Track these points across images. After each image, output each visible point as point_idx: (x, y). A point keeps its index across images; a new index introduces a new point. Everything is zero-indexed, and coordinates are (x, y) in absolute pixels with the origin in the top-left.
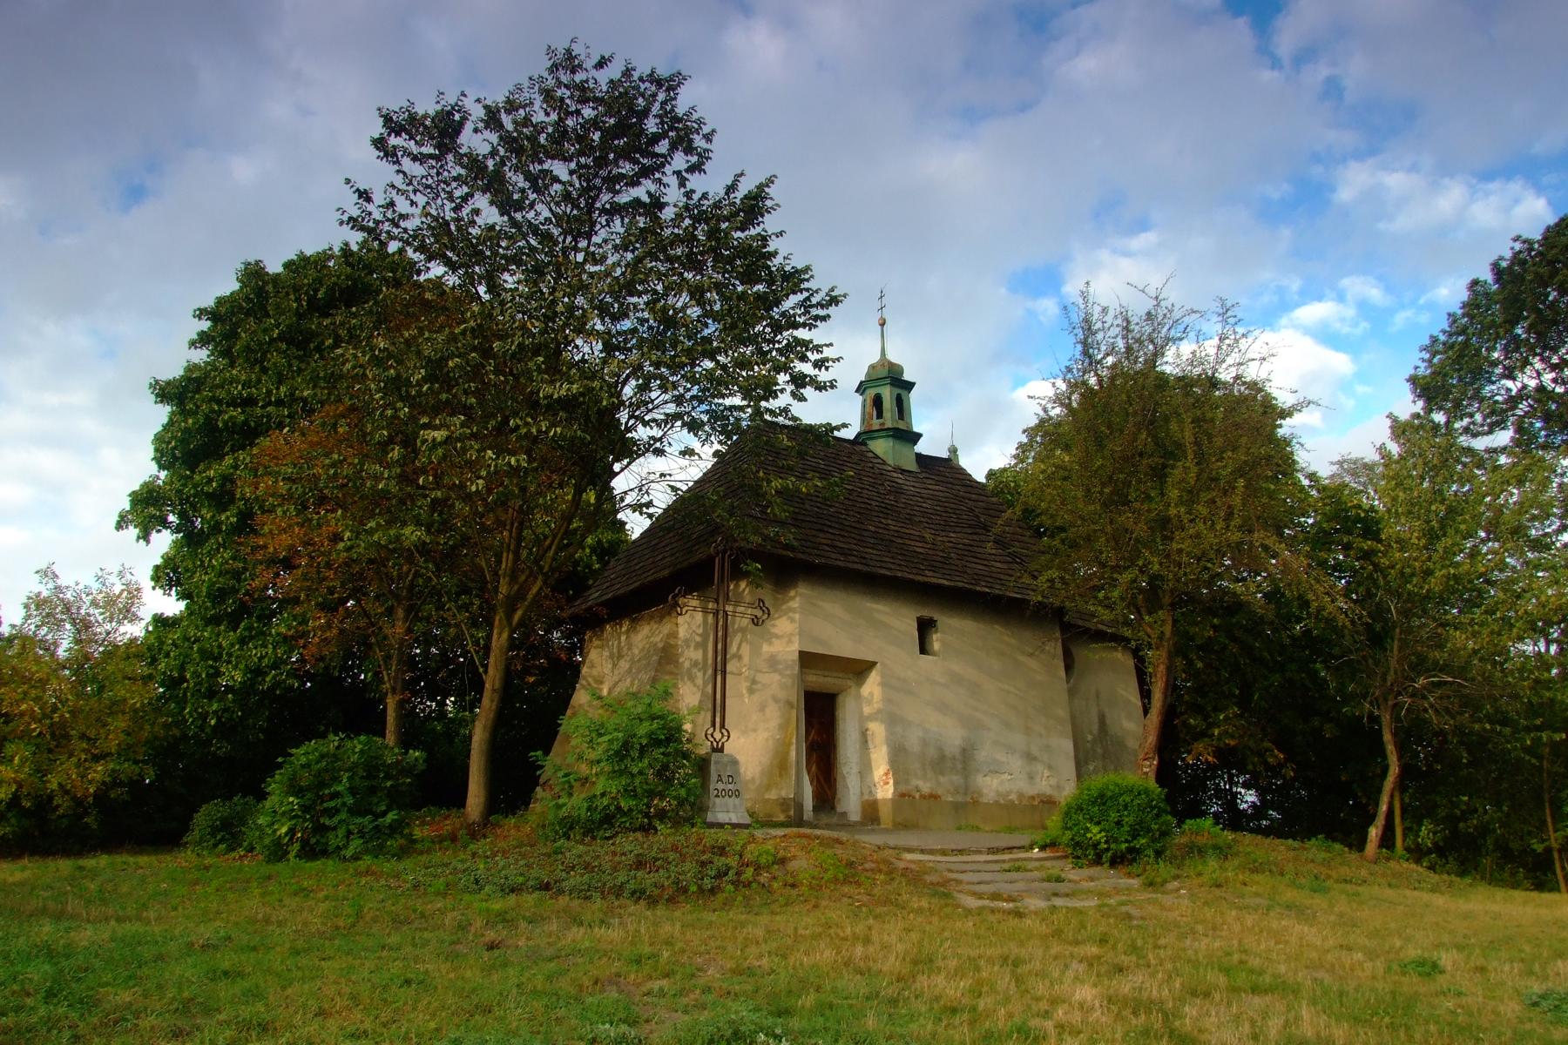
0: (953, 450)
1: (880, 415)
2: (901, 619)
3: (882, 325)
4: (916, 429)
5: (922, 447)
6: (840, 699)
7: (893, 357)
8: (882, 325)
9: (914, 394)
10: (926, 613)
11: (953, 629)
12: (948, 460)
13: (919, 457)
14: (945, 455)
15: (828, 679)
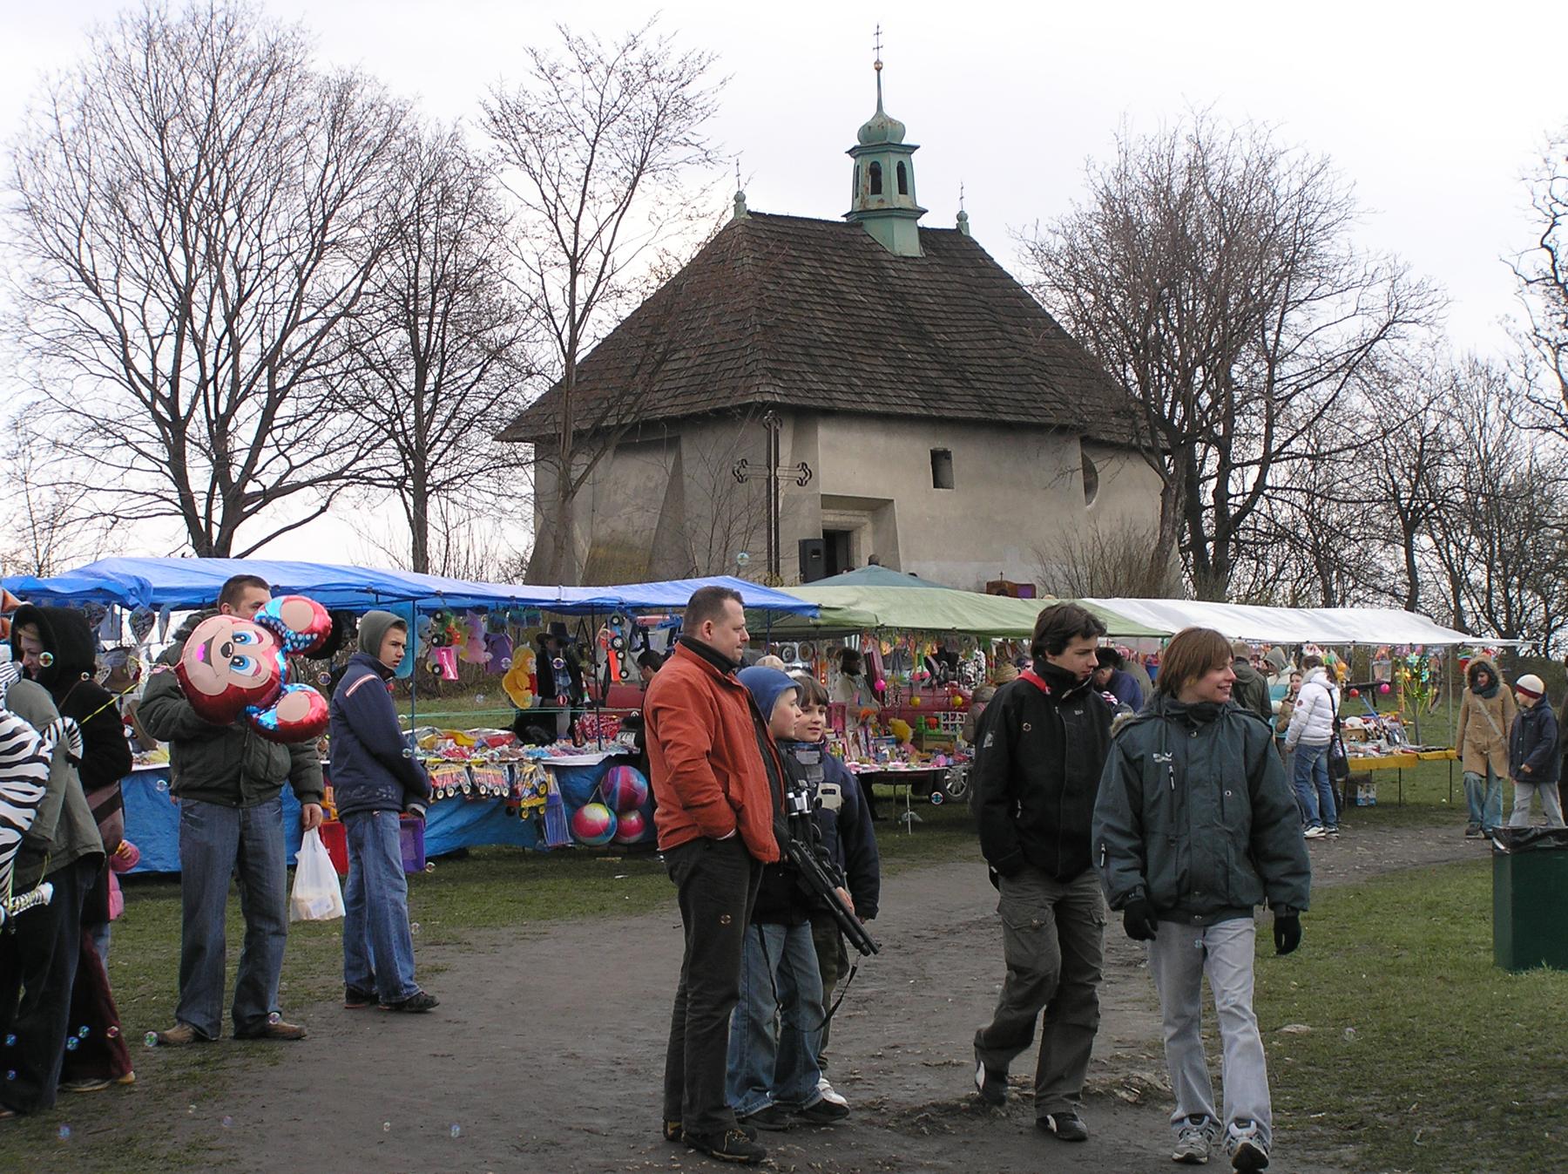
0: (962, 217)
1: (877, 188)
2: (914, 449)
3: (879, 70)
4: (921, 204)
5: (924, 222)
6: (855, 535)
7: (890, 111)
8: (879, 70)
9: (915, 156)
10: (940, 445)
11: (967, 456)
12: (957, 231)
13: (922, 230)
14: (951, 224)
15: (844, 518)
